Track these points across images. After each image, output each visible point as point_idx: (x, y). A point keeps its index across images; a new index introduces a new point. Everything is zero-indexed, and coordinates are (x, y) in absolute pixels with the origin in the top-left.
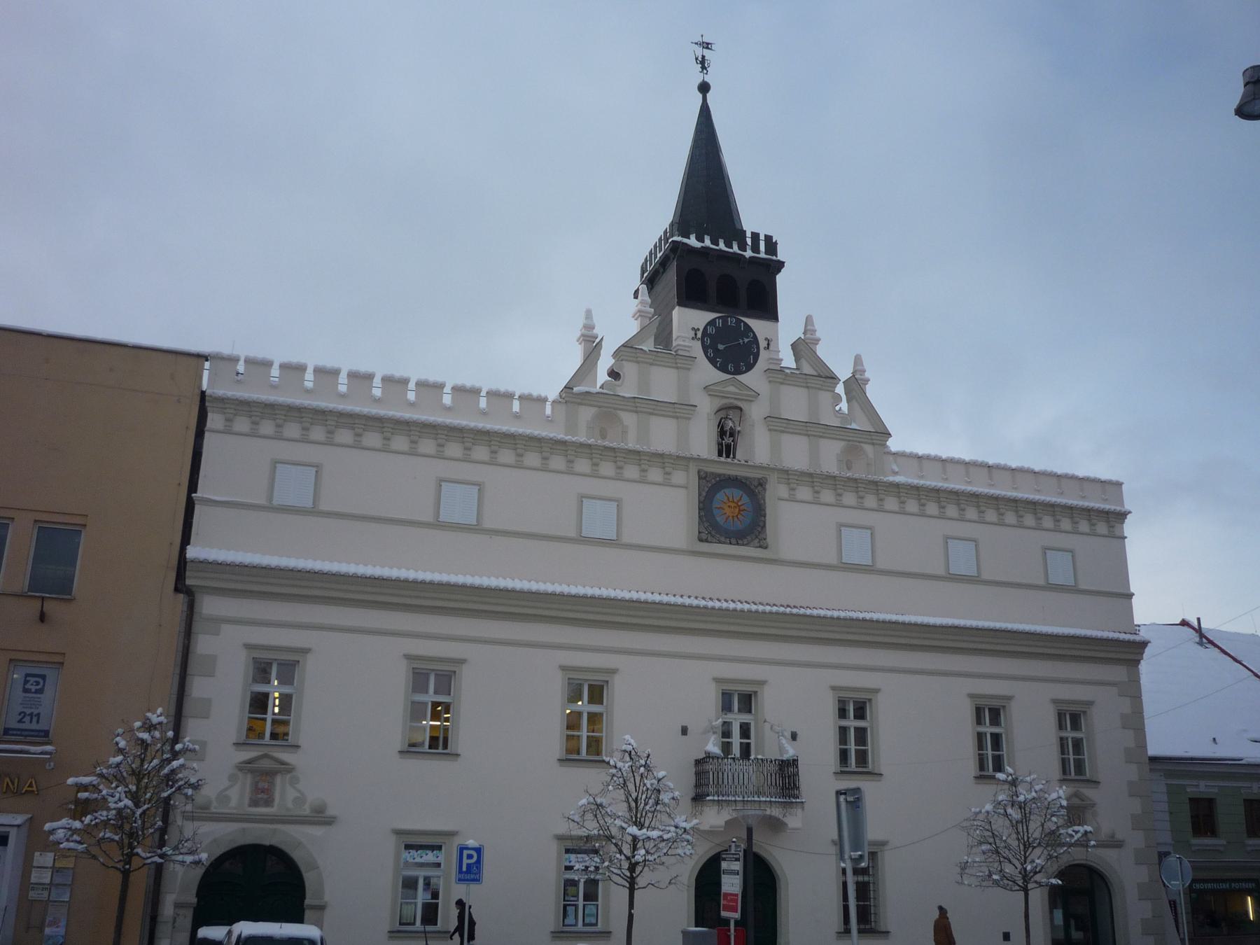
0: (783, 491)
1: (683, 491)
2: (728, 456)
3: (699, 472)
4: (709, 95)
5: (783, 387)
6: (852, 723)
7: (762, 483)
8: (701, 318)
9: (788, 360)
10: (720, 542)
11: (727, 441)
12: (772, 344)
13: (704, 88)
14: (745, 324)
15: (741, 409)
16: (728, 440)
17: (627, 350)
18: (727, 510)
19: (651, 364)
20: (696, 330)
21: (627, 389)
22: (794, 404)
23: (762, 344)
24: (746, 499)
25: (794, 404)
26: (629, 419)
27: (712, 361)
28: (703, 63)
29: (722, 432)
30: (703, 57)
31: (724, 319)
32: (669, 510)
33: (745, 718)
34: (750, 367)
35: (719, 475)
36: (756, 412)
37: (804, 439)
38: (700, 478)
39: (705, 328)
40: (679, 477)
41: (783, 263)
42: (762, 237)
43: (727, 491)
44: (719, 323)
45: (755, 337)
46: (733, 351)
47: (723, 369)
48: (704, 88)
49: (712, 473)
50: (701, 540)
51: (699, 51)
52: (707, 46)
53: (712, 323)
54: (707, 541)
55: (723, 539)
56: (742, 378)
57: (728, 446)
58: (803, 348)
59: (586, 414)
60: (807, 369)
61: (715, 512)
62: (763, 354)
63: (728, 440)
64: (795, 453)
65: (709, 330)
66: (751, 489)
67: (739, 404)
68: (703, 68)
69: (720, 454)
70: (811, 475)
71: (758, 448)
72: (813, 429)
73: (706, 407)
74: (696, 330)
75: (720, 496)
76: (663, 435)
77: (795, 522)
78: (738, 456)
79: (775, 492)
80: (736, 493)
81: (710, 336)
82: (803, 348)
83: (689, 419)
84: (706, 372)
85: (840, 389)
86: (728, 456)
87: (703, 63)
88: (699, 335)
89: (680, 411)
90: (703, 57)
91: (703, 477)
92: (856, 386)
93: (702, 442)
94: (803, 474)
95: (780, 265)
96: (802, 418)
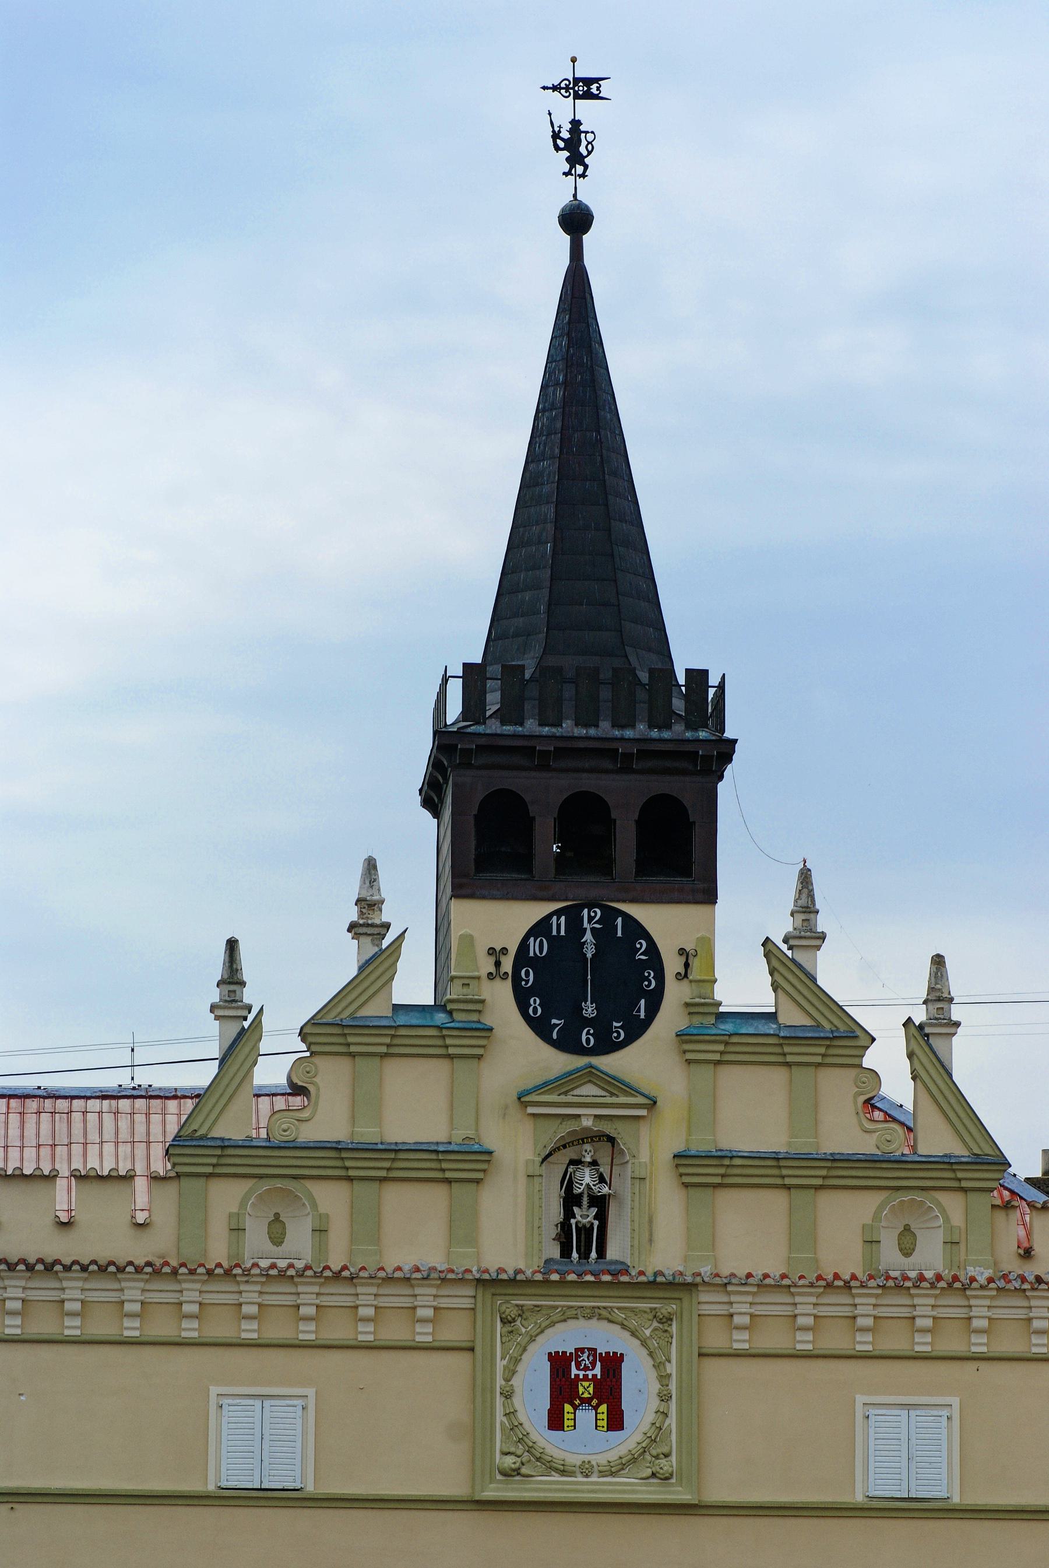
1: (461, 1361)
2: (585, 1255)
5: (725, 1071)
9: (743, 986)
12: (695, 963)
13: (576, 221)
14: (628, 918)
15: (611, 1140)
16: (584, 1215)
17: (331, 1032)
20: (496, 954)
21: (329, 1121)
22: (753, 1112)
23: (672, 965)
25: (753, 1112)
26: (331, 1199)
27: (540, 1027)
28: (573, 146)
29: (570, 1200)
30: (576, 124)
31: (573, 915)
34: (636, 1029)
37: (778, 1200)
39: (523, 946)
44: (560, 926)
45: (653, 949)
46: (593, 991)
47: (568, 1044)
48: (576, 221)
51: (564, 109)
52: (585, 88)
53: (540, 928)
56: (607, 1062)
57: (585, 1231)
59: (226, 1197)
60: (792, 1017)
62: (675, 993)
63: (584, 1215)
65: (534, 947)
67: (608, 1128)
68: (576, 159)
69: (566, 1253)
72: (801, 1173)
74: (496, 954)
78: (612, 1253)
81: (534, 963)
84: (521, 1054)
86: (585, 1255)
87: (573, 146)
88: (507, 965)
90: (576, 124)
92: (929, 1038)
93: (511, 1227)
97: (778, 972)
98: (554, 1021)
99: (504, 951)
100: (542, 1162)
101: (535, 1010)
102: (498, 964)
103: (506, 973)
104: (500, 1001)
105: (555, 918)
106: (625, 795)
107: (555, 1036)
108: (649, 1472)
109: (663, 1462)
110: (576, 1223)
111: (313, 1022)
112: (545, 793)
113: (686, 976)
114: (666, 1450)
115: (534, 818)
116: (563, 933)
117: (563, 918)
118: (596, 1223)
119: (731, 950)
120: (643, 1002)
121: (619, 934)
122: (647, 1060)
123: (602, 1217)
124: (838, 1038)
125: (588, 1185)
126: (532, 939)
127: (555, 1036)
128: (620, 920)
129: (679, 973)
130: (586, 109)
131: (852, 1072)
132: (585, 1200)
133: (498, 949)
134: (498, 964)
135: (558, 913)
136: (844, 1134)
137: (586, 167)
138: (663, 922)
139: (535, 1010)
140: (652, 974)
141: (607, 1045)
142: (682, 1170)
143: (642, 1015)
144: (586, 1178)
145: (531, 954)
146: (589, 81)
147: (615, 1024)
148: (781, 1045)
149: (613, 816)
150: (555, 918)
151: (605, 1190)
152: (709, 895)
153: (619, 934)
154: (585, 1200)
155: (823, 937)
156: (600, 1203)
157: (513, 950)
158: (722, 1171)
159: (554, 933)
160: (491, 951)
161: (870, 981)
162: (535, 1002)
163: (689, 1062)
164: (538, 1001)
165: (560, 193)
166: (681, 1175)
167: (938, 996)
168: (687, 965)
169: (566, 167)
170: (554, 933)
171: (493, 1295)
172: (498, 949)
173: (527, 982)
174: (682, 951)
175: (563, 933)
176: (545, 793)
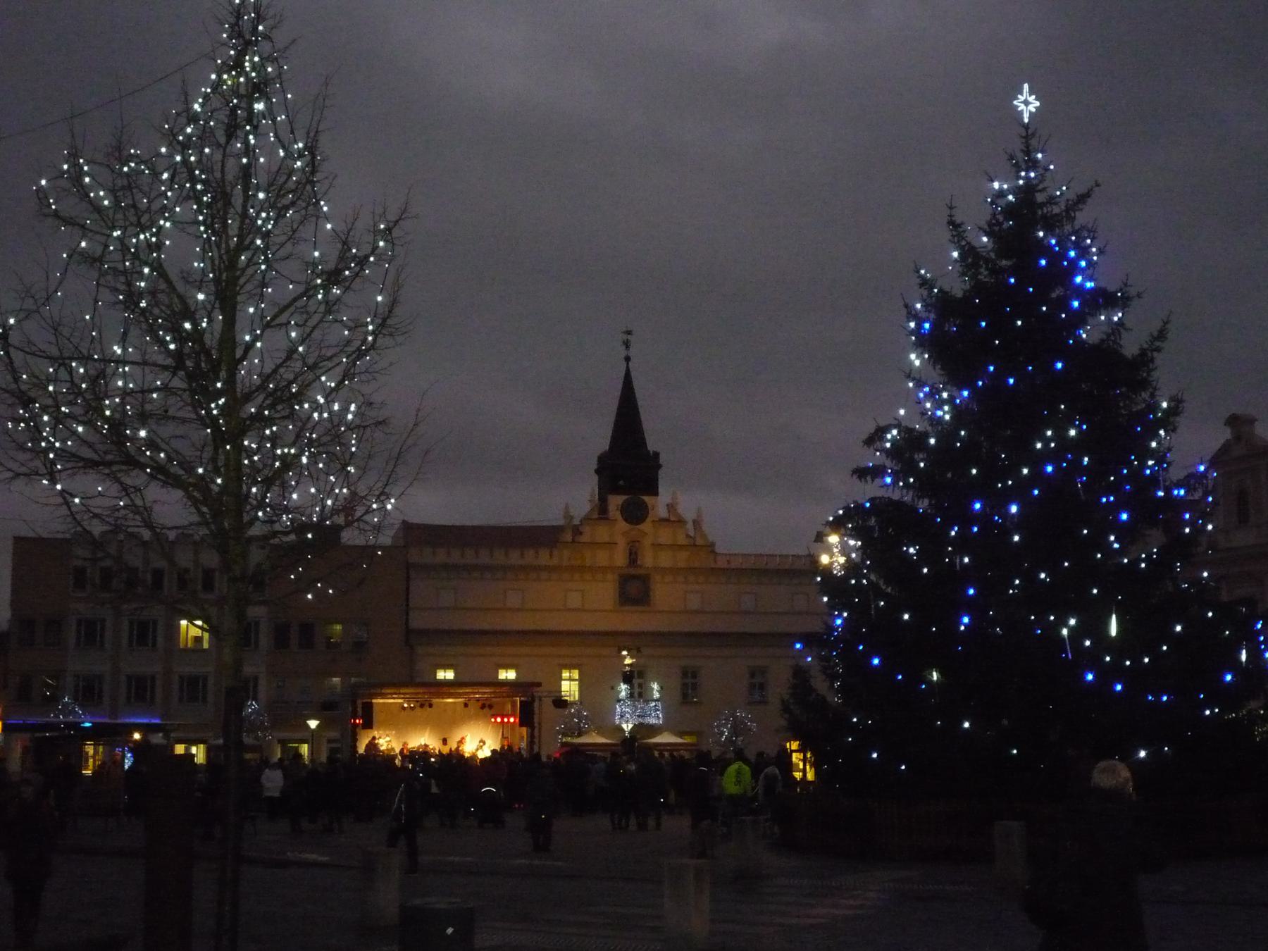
6: (690, 681)
11: (633, 557)
13: (628, 359)
25: (665, 536)
27: (626, 520)
28: (627, 344)
32: (603, 592)
33: (641, 681)
36: (647, 542)
40: (610, 577)
46: (636, 514)
48: (628, 359)
51: (625, 337)
52: (629, 333)
58: (671, 507)
64: (665, 560)
66: (645, 580)
71: (648, 560)
73: (622, 544)
76: (602, 558)
77: (664, 593)
82: (671, 507)
84: (622, 525)
85: (690, 526)
87: (627, 344)
89: (611, 545)
91: (621, 576)
92: (697, 523)
93: (620, 559)
95: (659, 466)
96: (669, 542)
119: (659, 505)
122: (646, 526)
124: (681, 522)
136: (681, 540)
141: (638, 524)
152: (656, 493)
161: (688, 513)
165: (623, 353)
167: (699, 514)
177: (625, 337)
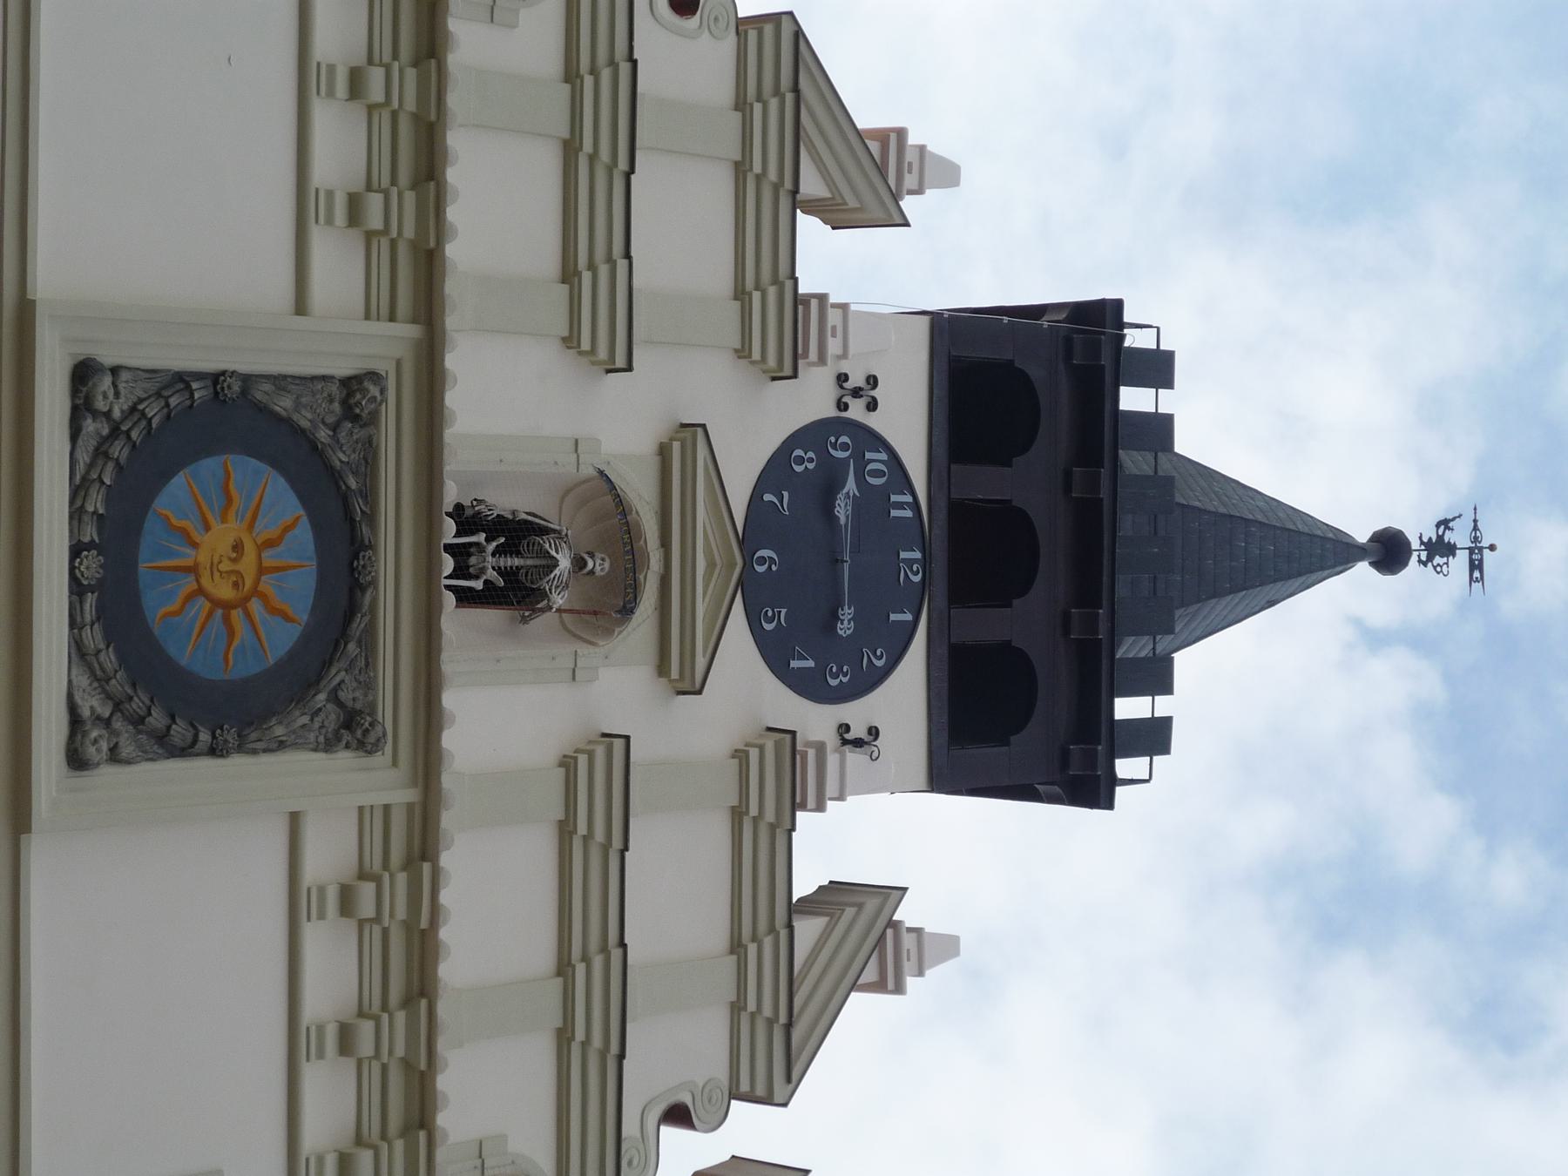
0: (329, 854)
3: (374, 376)
4: (1363, 569)
7: (353, 729)
8: (905, 422)
10: (78, 491)
13: (1389, 551)
15: (627, 611)
18: (219, 539)
19: (740, 169)
22: (675, 891)
23: (857, 713)
24: (280, 639)
28: (1439, 548)
29: (517, 533)
34: (775, 653)
35: (369, 494)
36: (615, 685)
37: (539, 952)
38: (352, 385)
39: (879, 442)
41: (1110, 805)
42: (1163, 706)
43: (304, 534)
48: (1389, 551)
49: (369, 452)
50: (83, 373)
54: (81, 408)
55: (95, 502)
61: (209, 466)
65: (876, 458)
70: (422, 987)
75: (279, 501)
79: (329, 795)
80: (298, 588)
83: (570, 340)
84: (751, 429)
87: (1439, 548)
88: (856, 411)
91: (353, 395)
94: (423, 947)
95: (1091, 788)
97: (858, 914)
98: (786, 494)
99: (872, 406)
100: (601, 473)
101: (800, 460)
102: (856, 393)
103: (846, 407)
104: (809, 399)
105: (909, 499)
106: (1027, 622)
107: (768, 497)
108: (86, 713)
109: (104, 746)
110: (477, 544)
111: (798, 34)
112: (1029, 484)
113: (845, 742)
114: (127, 750)
115: (1010, 466)
116: (894, 513)
117: (908, 513)
118: (478, 585)
120: (811, 663)
121: (893, 617)
123: (488, 597)
125: (556, 565)
126: (883, 456)
127: (768, 497)
128: (908, 617)
129: (847, 728)
130: (1460, 561)
131: (722, 1073)
132: (517, 562)
133: (873, 393)
134: (856, 393)
135: (915, 505)
136: (649, 1073)
137: (1425, 564)
138: (902, 701)
139: (800, 460)
140: (845, 680)
142: (600, 752)
143: (794, 664)
144: (564, 563)
145: (868, 455)
146: (1480, 567)
147: (784, 611)
148: (772, 930)
149: (1016, 602)
150: (909, 499)
151: (559, 600)
153: (893, 617)
154: (517, 562)
155: (899, 989)
156: (517, 594)
157: (873, 421)
158: (599, 836)
159: (894, 498)
160: (873, 381)
162: (806, 462)
163: (740, 755)
164: (811, 466)
166: (591, 755)
168: (858, 743)
169: (1425, 540)
170: (894, 498)
171: (399, 363)
172: (873, 393)
173: (834, 446)
174: (874, 732)
175: (894, 513)
176: (1029, 484)
177: (1459, 536)
